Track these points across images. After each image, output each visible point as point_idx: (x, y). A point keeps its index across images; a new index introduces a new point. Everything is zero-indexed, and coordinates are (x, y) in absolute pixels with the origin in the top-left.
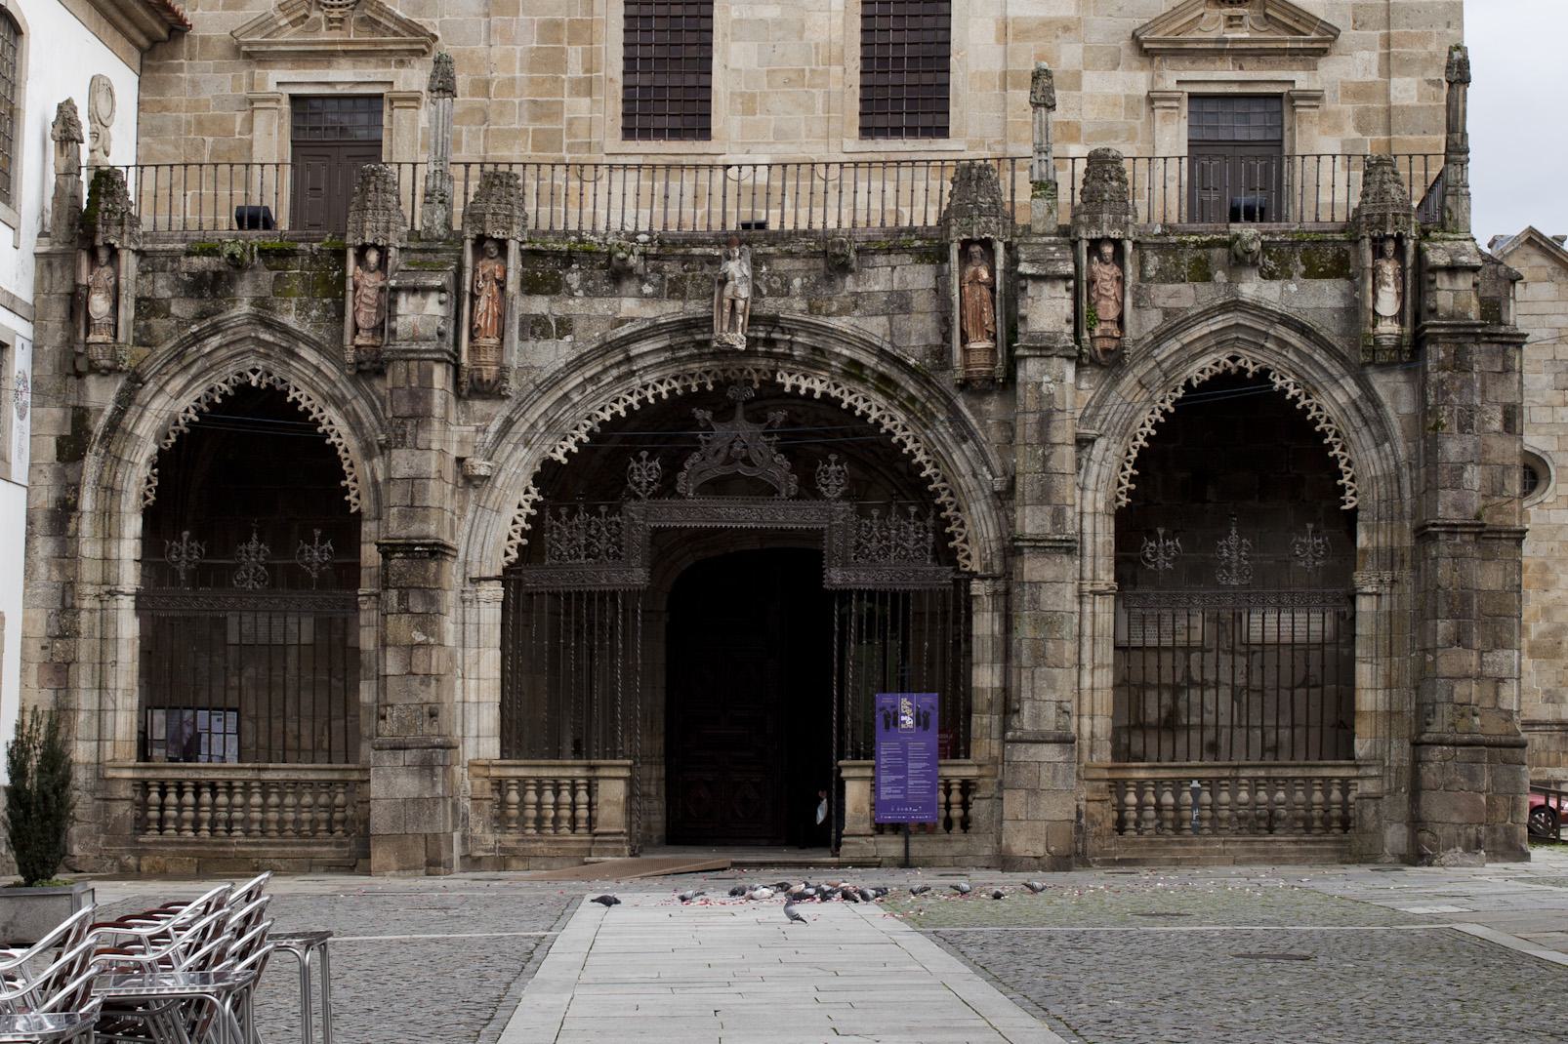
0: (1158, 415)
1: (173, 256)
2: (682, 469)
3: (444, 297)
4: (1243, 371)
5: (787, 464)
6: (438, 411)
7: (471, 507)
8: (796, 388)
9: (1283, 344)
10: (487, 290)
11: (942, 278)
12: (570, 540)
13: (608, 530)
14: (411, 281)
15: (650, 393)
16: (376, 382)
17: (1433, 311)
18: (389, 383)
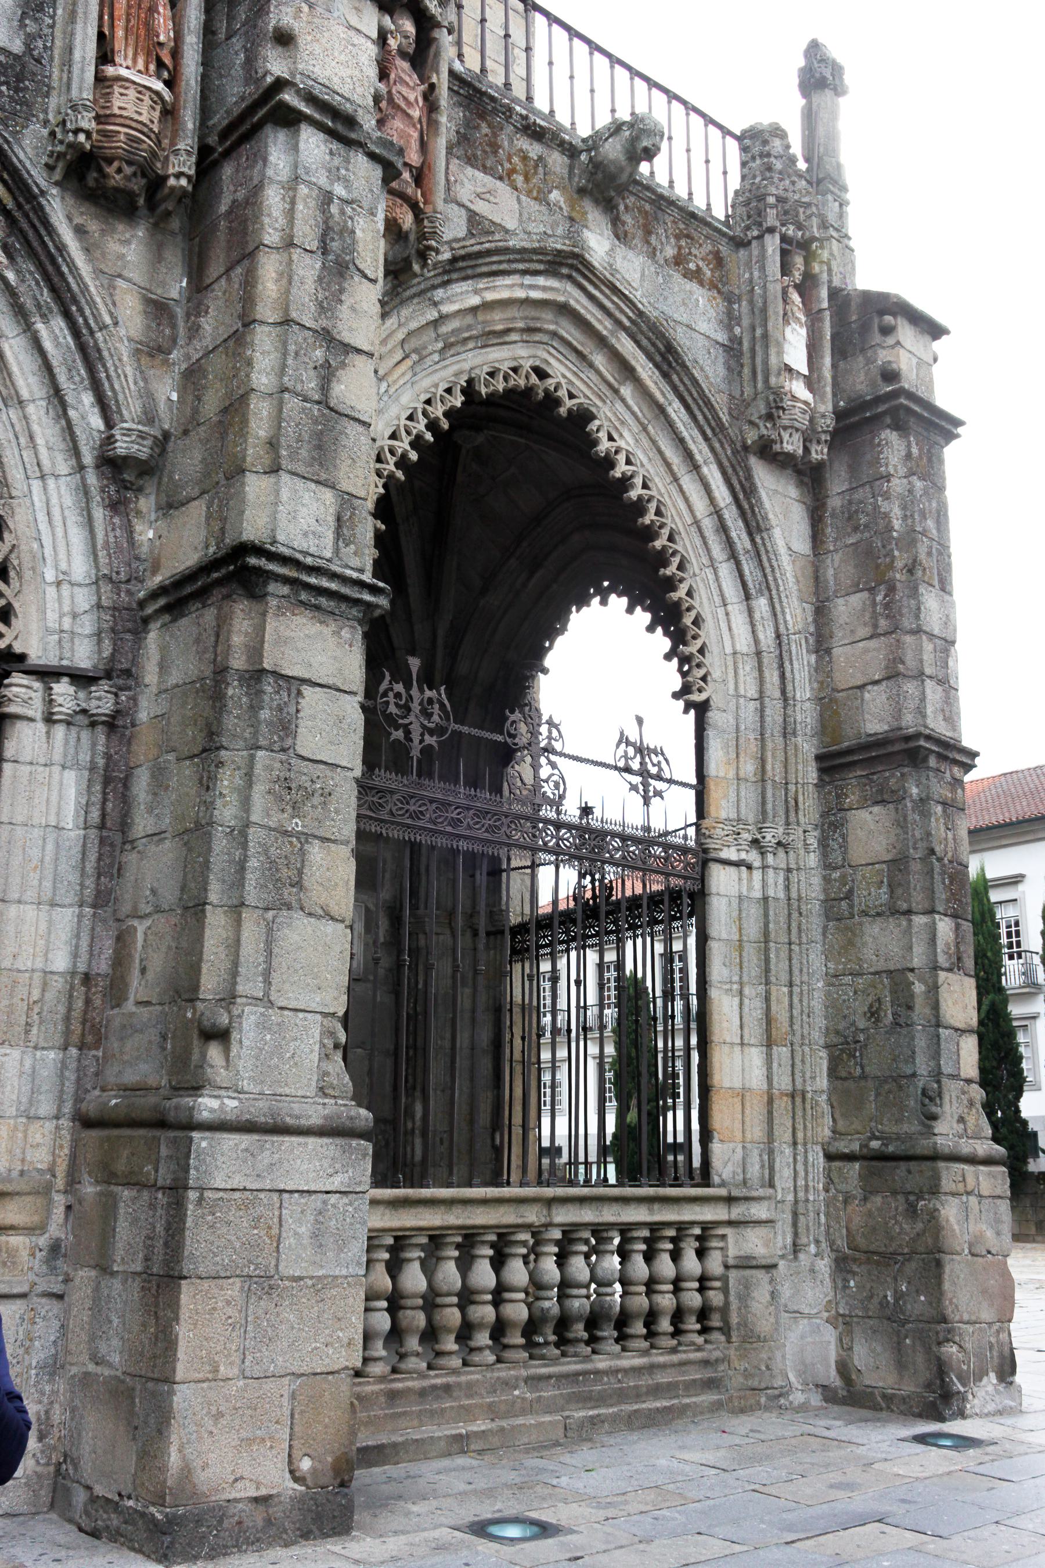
0: (421, 425)
4: (551, 401)
9: (627, 370)
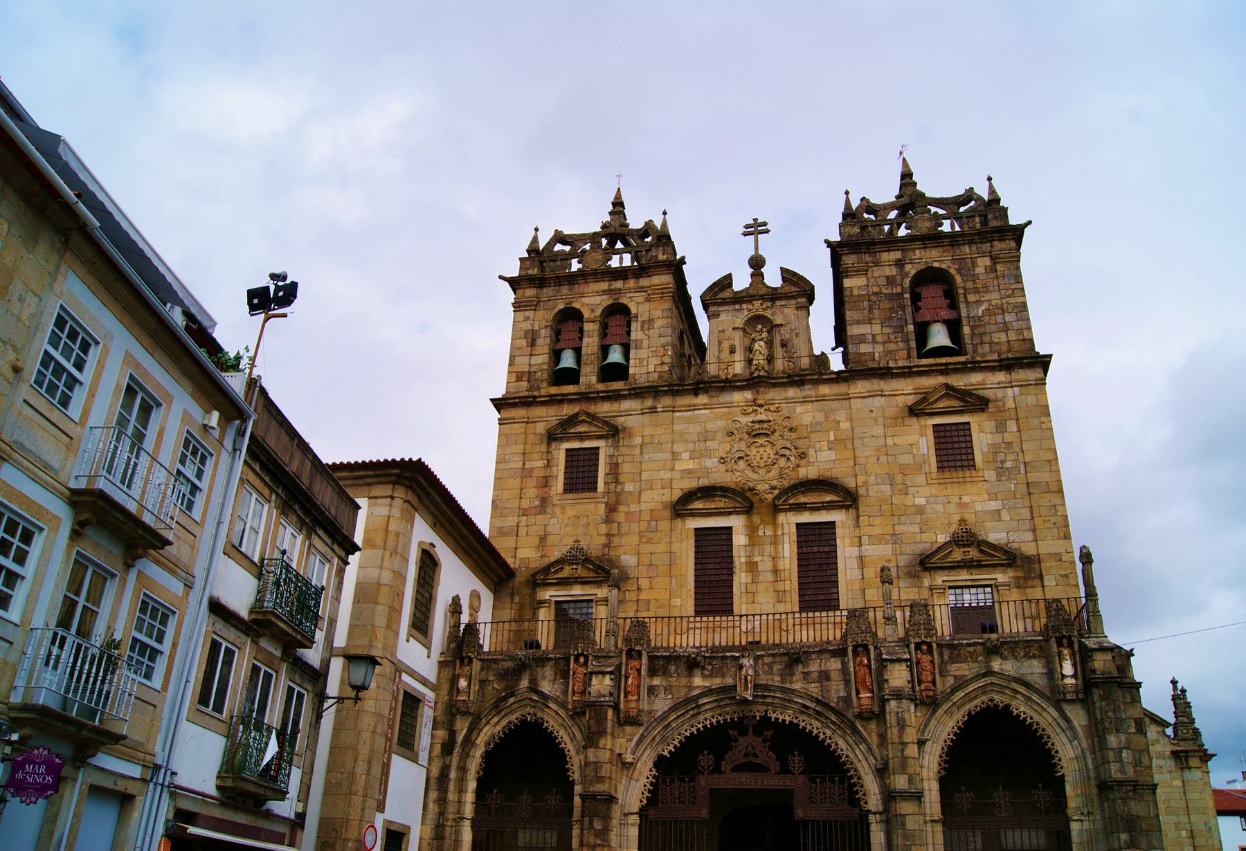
1: (496, 661)
2: (724, 759)
3: (612, 676)
4: (996, 706)
5: (774, 756)
6: (609, 730)
7: (625, 777)
8: (777, 719)
9: (1017, 692)
10: (633, 673)
11: (844, 664)
12: (671, 795)
13: (689, 789)
14: (598, 669)
15: (708, 722)
16: (582, 718)
17: (1094, 671)
18: (587, 717)
